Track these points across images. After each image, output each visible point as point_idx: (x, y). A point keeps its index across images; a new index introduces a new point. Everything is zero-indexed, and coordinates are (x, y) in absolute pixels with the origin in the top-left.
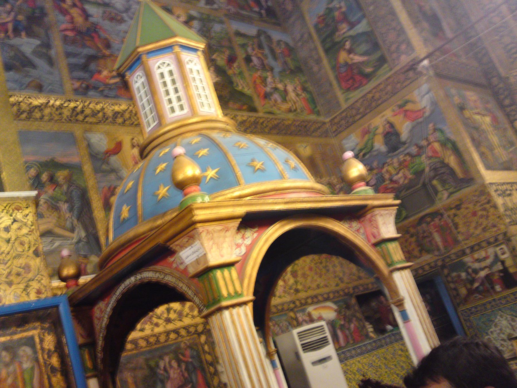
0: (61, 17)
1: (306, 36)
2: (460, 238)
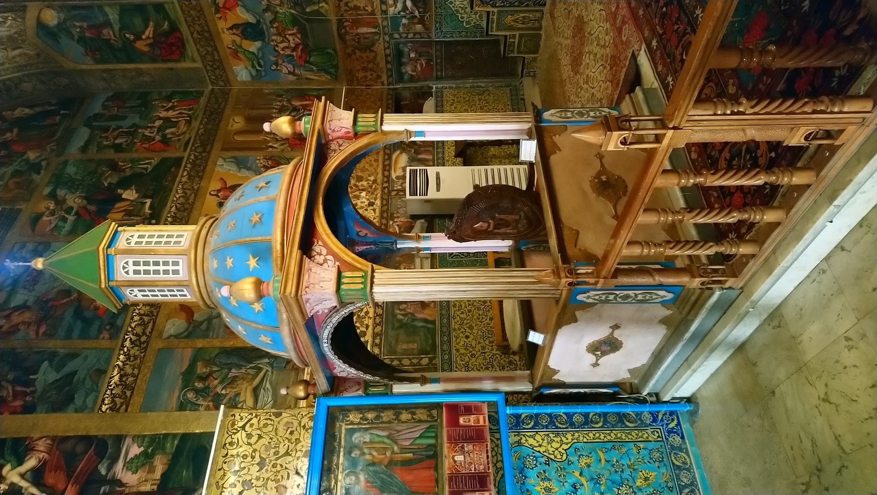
0: (20, 335)
1: (105, 75)
2: (369, 9)
